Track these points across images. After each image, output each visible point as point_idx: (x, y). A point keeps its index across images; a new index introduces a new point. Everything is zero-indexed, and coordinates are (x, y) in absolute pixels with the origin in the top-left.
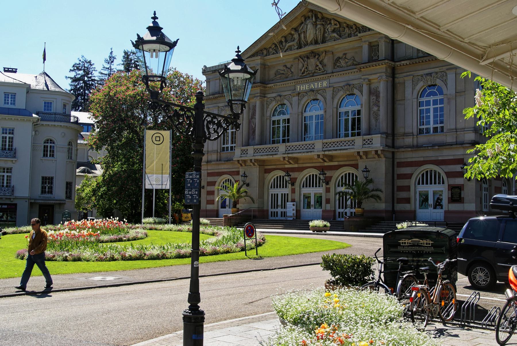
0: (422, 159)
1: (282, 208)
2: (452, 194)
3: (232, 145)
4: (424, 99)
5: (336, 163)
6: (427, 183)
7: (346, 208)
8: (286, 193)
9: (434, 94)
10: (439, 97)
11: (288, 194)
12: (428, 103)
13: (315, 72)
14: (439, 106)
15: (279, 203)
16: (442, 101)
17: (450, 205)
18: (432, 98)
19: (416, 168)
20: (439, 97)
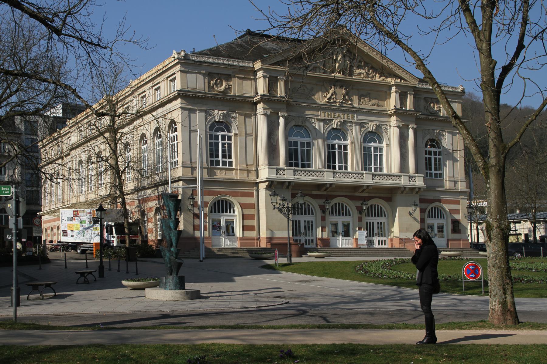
0: (432, 198)
1: (306, 235)
2: (453, 226)
3: (224, 160)
4: (428, 149)
5: (367, 195)
6: (432, 217)
7: (373, 236)
8: (310, 220)
9: (434, 147)
10: (437, 150)
11: (312, 222)
12: (430, 153)
13: (342, 102)
14: (437, 157)
15: (302, 230)
16: (440, 153)
17: (453, 234)
18: (433, 150)
19: (428, 204)
20: (437, 150)
